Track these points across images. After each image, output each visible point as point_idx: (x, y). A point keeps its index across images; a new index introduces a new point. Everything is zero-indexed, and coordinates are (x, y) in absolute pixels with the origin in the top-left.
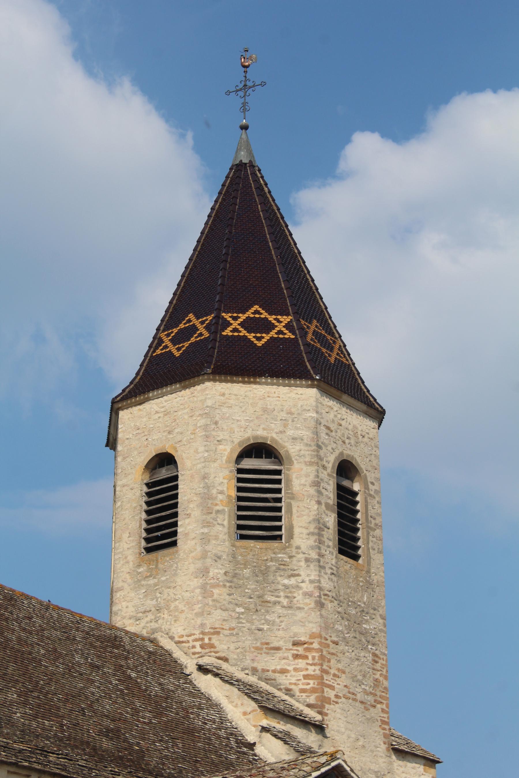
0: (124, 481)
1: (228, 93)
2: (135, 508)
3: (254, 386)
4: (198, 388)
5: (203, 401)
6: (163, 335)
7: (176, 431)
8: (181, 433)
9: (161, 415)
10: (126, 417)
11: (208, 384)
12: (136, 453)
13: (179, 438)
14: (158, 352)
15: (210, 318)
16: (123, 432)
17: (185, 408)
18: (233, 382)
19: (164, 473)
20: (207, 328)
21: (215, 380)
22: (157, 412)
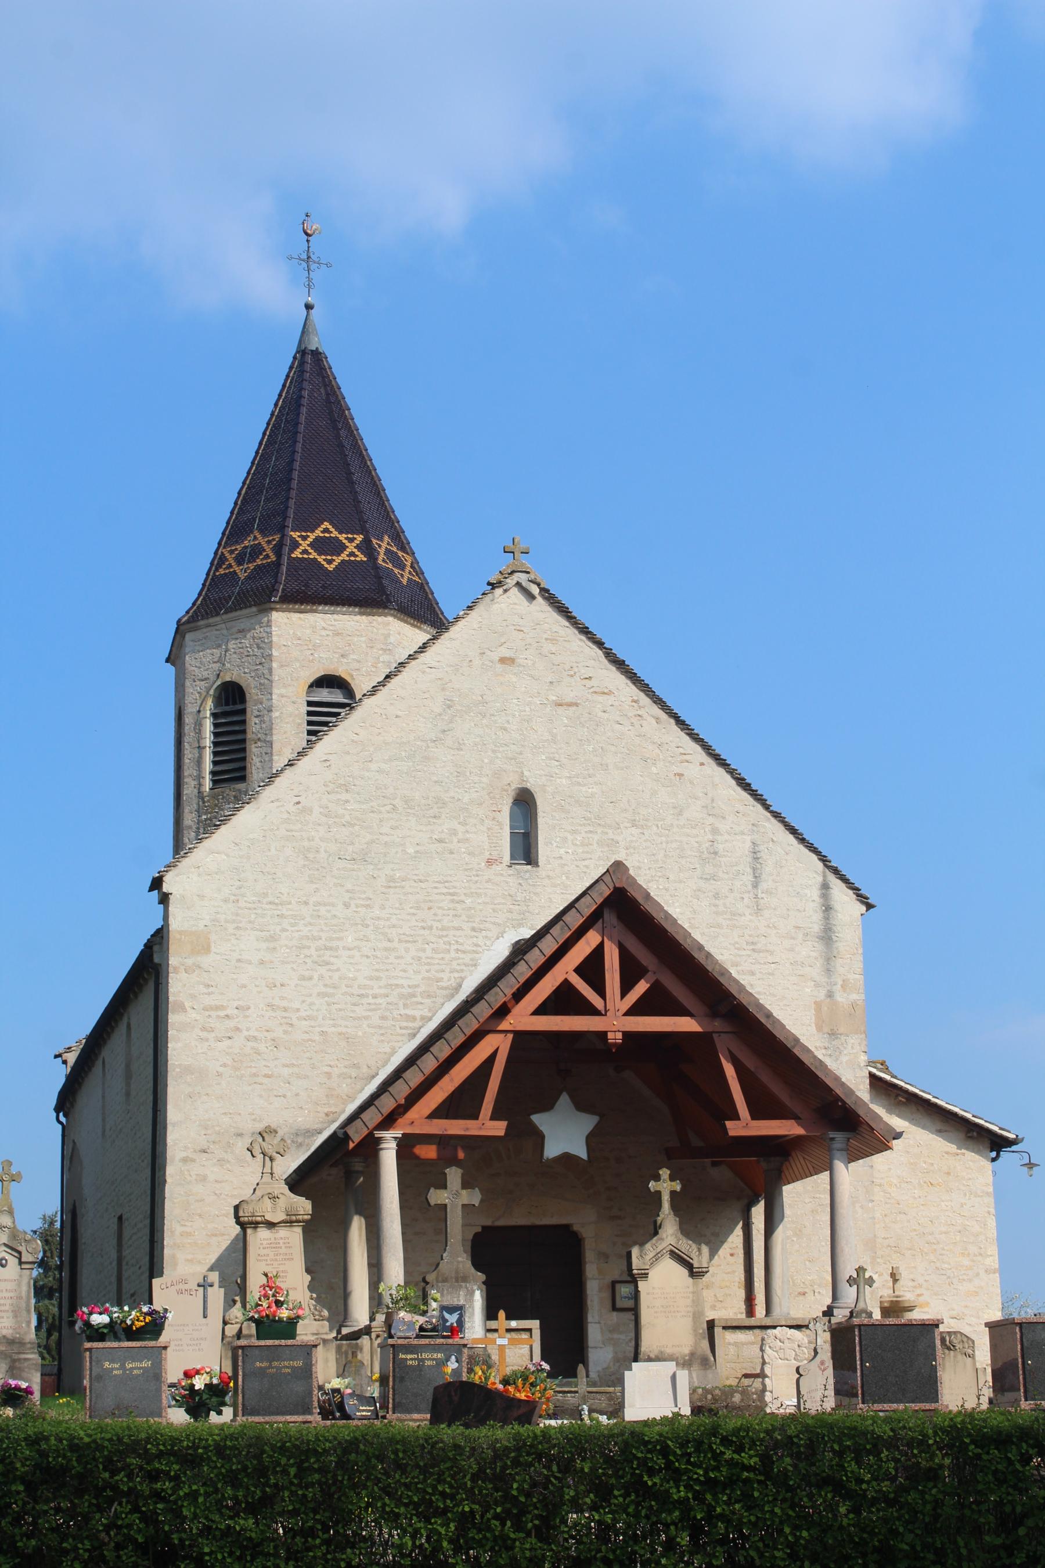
0: (283, 691)
1: (290, 258)
2: (299, 724)
3: (417, 631)
4: (380, 619)
5: (389, 635)
6: (295, 535)
7: (352, 656)
8: (359, 662)
9: (330, 633)
10: (280, 620)
11: (390, 619)
12: (298, 665)
13: (356, 665)
14: (297, 554)
15: (359, 538)
16: (279, 636)
17: (361, 636)
18: (406, 622)
19: (325, 695)
20: (357, 547)
21: (395, 617)
22: (324, 628)
